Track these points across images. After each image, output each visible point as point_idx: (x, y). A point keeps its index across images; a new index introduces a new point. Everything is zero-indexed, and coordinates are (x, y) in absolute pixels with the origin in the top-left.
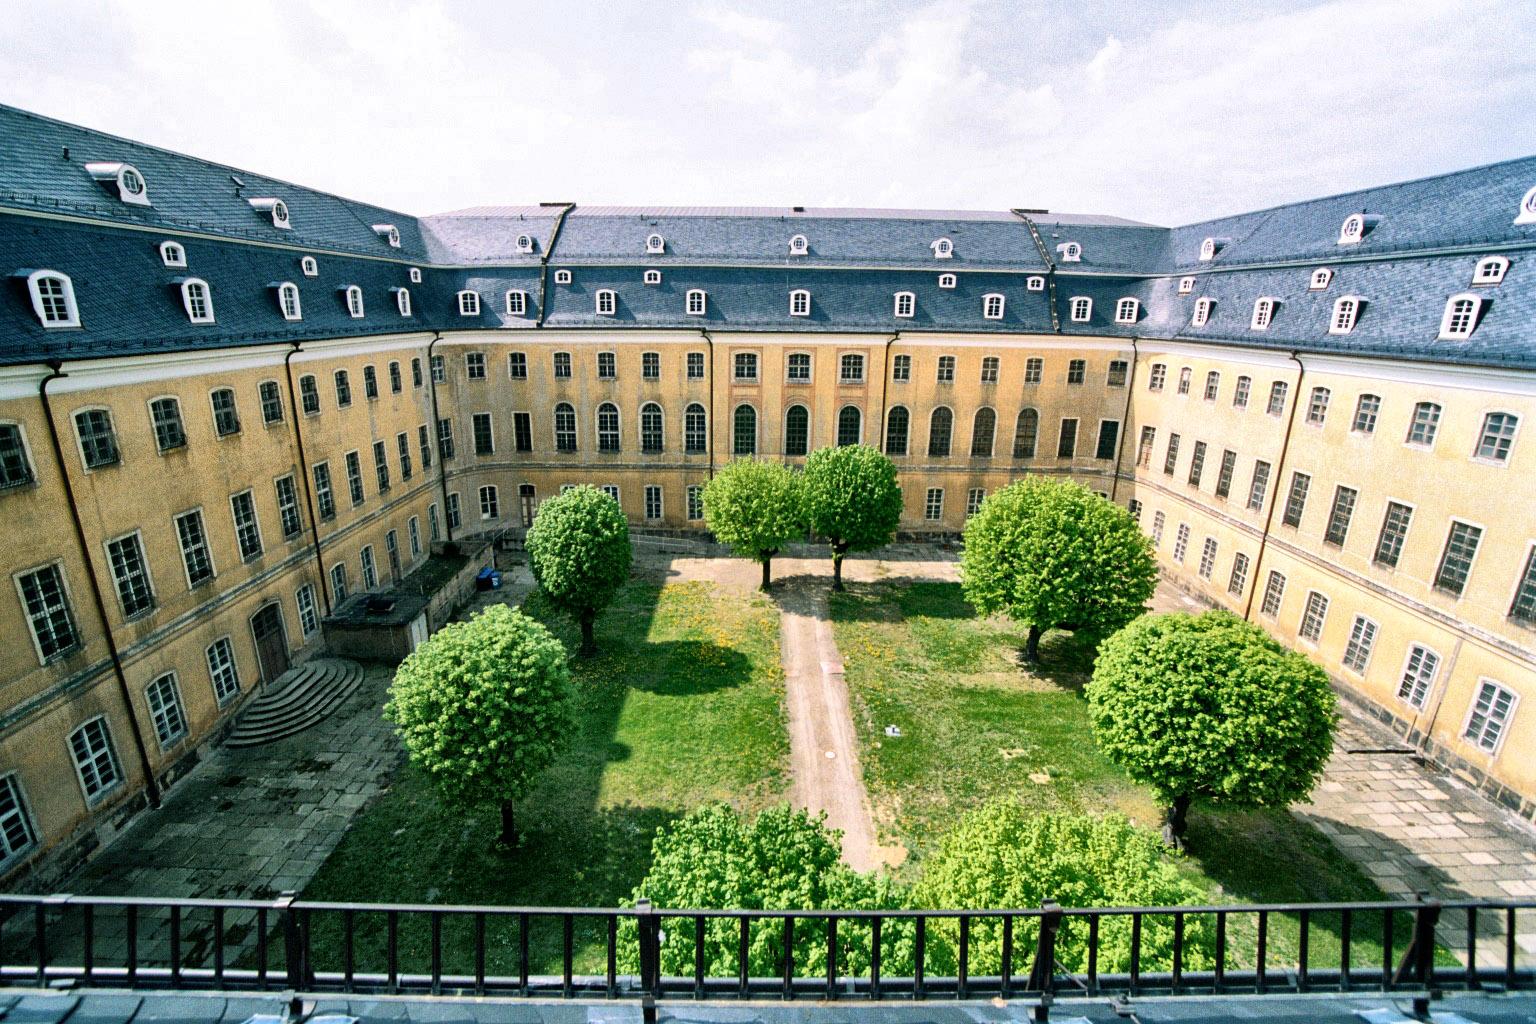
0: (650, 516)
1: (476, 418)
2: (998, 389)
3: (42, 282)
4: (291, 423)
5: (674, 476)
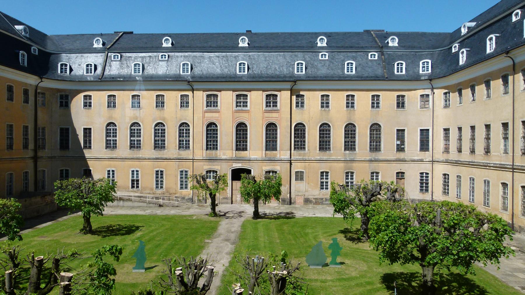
0: (157, 187)
1: (62, 129)
2: (356, 112)
5: (173, 165)
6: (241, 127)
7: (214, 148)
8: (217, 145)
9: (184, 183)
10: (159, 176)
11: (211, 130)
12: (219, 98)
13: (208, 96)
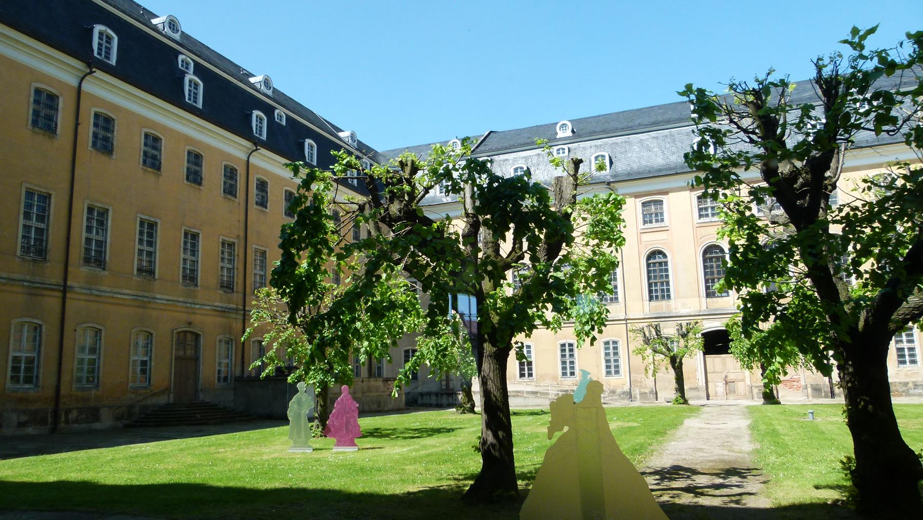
0: (564, 374)
3: (101, 34)
4: (243, 203)
6: (711, 253)
7: (663, 297)
8: (668, 290)
9: (613, 364)
10: (567, 353)
11: (654, 264)
12: (665, 206)
13: (644, 204)
